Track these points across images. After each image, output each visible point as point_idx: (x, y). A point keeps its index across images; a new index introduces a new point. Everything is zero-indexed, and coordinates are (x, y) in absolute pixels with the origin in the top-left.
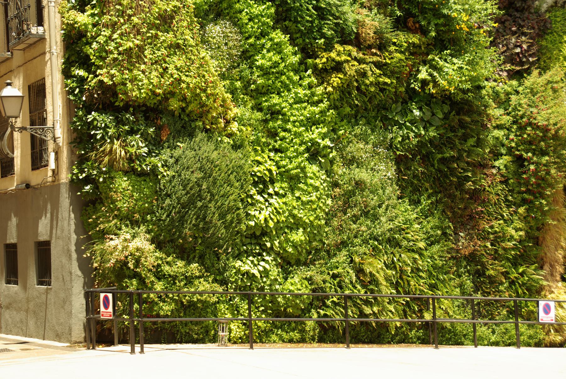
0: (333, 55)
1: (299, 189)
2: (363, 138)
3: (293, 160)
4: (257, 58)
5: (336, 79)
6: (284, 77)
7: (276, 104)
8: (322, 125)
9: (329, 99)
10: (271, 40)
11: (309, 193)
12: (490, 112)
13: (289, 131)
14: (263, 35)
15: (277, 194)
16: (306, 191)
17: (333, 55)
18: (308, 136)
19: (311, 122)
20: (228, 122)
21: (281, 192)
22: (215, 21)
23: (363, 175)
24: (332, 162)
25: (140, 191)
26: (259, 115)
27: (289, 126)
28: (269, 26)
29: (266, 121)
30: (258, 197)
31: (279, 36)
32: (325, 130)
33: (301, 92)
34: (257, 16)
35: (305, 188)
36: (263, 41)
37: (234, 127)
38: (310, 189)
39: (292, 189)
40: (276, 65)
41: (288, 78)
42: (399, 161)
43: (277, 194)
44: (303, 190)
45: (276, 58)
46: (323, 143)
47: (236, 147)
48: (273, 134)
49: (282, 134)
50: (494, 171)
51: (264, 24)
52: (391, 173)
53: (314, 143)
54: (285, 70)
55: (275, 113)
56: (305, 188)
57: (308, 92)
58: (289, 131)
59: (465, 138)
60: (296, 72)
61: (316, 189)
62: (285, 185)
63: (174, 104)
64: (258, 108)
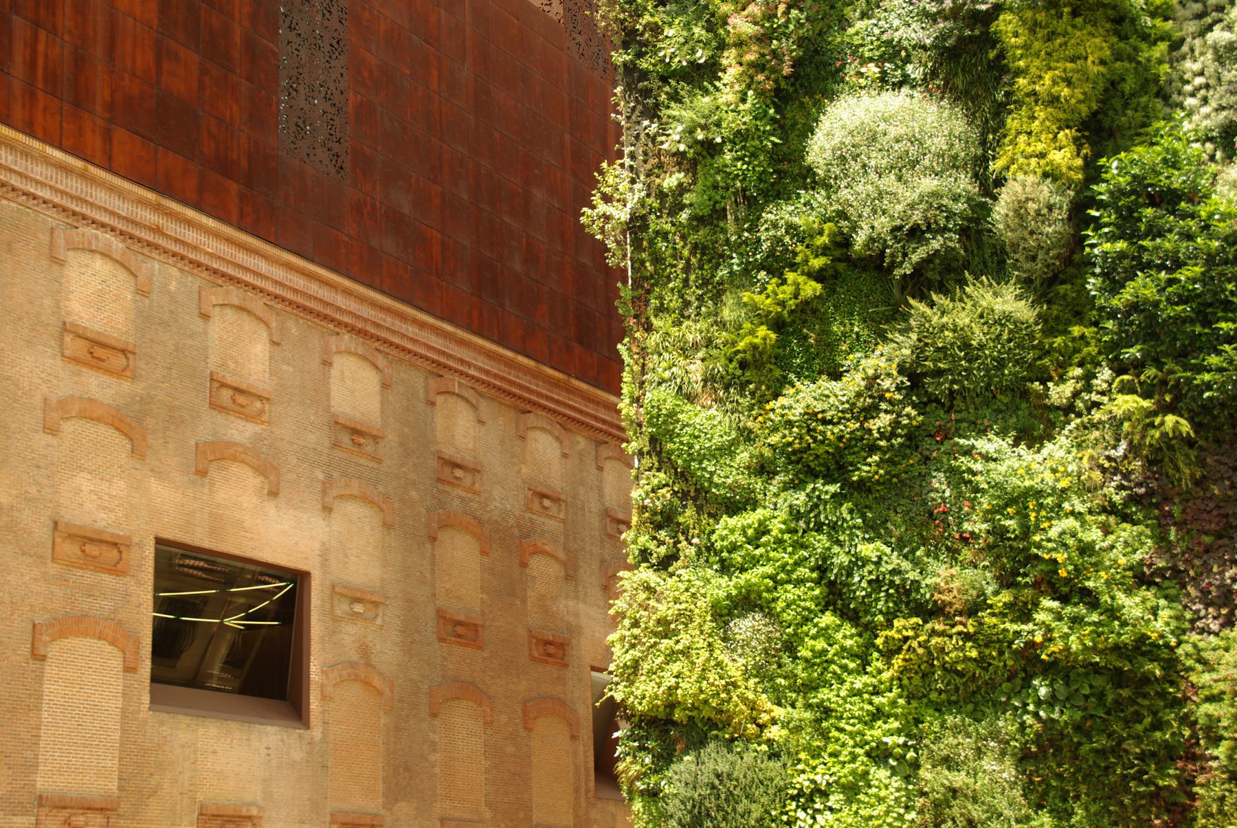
0: (892, 633)
1: (859, 801)
2: (956, 730)
3: (847, 765)
4: (800, 648)
5: (898, 661)
6: (833, 667)
7: (823, 701)
8: (892, 720)
9: (900, 686)
10: (816, 625)
11: (872, 806)
12: (1193, 678)
13: (841, 730)
14: (806, 620)
15: (831, 809)
16: (868, 803)
17: (892, 633)
18: (869, 734)
19: (879, 714)
20: (762, 727)
21: (837, 806)
22: (742, 616)
23: (959, 779)
24: (916, 765)
25: (651, 814)
26: (808, 715)
27: (842, 724)
28: (811, 611)
29: (818, 721)
30: (801, 814)
31: (828, 619)
32: (894, 724)
33: (859, 682)
34: (794, 602)
35: (867, 799)
36: (805, 628)
37: (775, 732)
38: (873, 800)
39: (849, 801)
40: (824, 652)
41: (841, 667)
42: (1023, 758)
43: (831, 809)
44: (863, 803)
45: (820, 644)
46: (890, 740)
47: (774, 756)
48: (825, 735)
49: (834, 733)
50: (1214, 764)
51: (804, 609)
52: (1008, 771)
53: (880, 743)
54: (836, 658)
55: (827, 712)
56: (867, 799)
57: (874, 680)
58: (841, 730)
59: (1138, 718)
60: (853, 656)
61: (881, 800)
62: (841, 796)
63: (678, 715)
64: (808, 706)
